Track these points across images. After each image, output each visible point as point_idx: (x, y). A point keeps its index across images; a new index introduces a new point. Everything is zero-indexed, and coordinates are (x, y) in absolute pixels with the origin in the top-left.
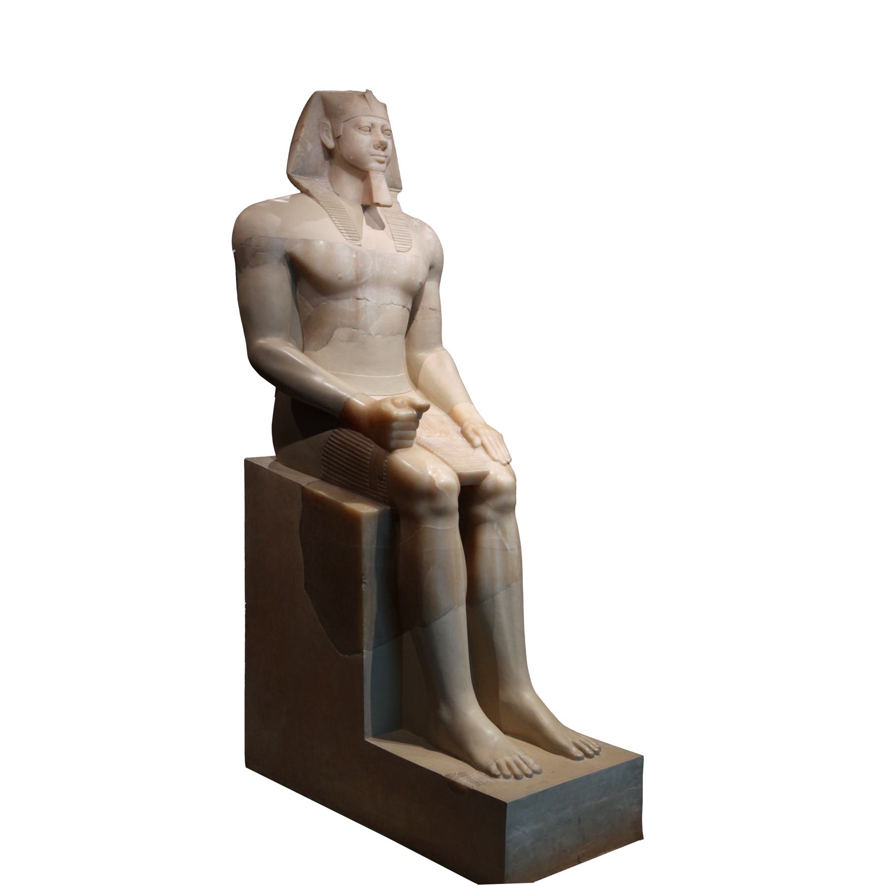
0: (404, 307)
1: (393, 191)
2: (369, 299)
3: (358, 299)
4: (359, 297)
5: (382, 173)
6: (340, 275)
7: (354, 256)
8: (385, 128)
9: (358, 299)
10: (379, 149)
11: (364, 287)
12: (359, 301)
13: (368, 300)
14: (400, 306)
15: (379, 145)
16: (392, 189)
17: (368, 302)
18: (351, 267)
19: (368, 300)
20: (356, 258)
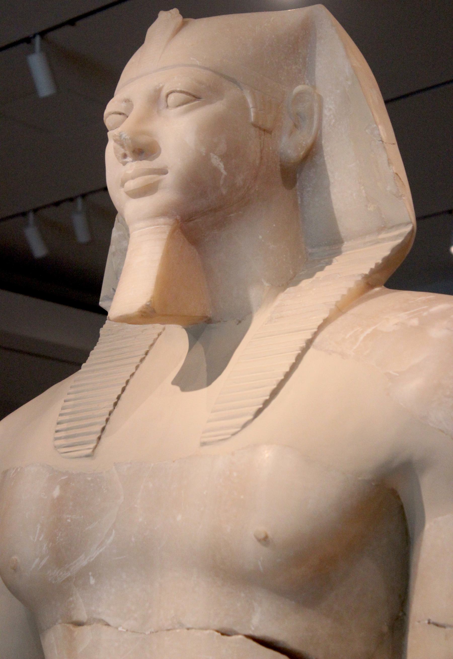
0: (224, 633)
1: (384, 240)
2: (107, 619)
3: (79, 624)
4: (75, 619)
5: (141, 224)
6: (15, 557)
7: (56, 492)
8: (164, 93)
9: (79, 624)
10: (129, 159)
11: (92, 581)
12: (78, 630)
13: (108, 625)
14: (208, 632)
15: (122, 151)
16: (383, 235)
17: (105, 628)
18: (39, 526)
19: (108, 625)
20: (60, 498)
